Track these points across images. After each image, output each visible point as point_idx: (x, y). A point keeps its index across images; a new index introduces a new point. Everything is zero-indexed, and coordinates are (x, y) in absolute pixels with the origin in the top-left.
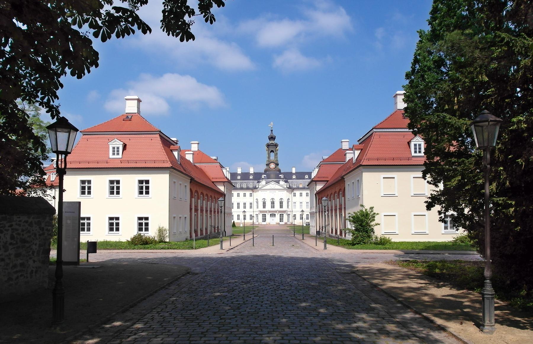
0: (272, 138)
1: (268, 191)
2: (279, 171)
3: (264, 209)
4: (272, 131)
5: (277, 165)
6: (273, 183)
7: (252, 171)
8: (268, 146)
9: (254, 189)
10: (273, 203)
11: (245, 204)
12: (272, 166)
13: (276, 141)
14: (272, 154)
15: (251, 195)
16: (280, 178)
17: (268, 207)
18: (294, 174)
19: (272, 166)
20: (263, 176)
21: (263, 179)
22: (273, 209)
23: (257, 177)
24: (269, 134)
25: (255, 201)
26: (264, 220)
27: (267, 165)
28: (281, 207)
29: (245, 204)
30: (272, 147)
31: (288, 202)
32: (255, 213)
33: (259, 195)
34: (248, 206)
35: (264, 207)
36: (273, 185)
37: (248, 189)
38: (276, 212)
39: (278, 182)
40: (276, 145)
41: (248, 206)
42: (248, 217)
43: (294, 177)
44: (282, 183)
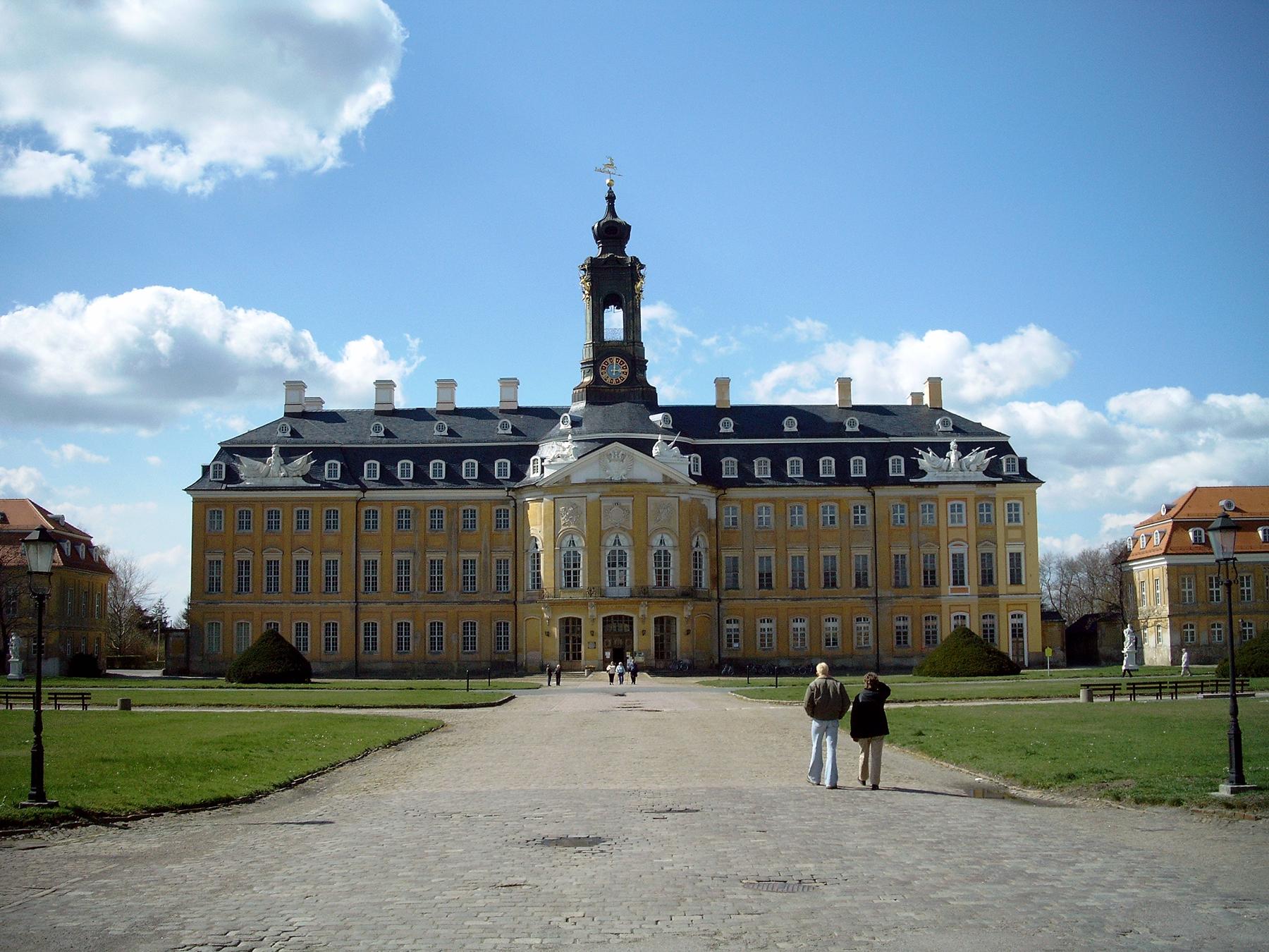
4: (611, 198)
5: (637, 364)
13: (631, 250)
14: (614, 319)
16: (653, 428)
19: (615, 371)
20: (564, 426)
21: (563, 435)
24: (599, 213)
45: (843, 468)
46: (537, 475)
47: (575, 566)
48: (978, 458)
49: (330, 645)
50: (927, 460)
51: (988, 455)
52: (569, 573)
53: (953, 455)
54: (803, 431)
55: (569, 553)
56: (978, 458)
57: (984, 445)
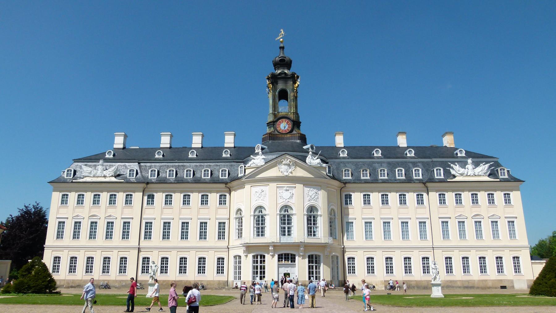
0: (284, 63)
1: (273, 185)
2: (303, 139)
5: (296, 124)
6: (289, 159)
8: (274, 79)
10: (286, 220)
11: (203, 225)
12: (284, 126)
13: (293, 69)
15: (222, 201)
17: (272, 233)
18: (341, 148)
19: (284, 126)
21: (258, 154)
22: (286, 239)
23: (242, 154)
25: (233, 215)
26: (259, 271)
27: (269, 124)
28: (311, 232)
29: (203, 225)
30: (282, 78)
31: (331, 223)
32: (233, 253)
34: (212, 230)
35: (260, 231)
36: (284, 168)
37: (215, 181)
38: (297, 246)
39: (303, 159)
40: (294, 78)
41: (212, 230)
42: (211, 265)
43: (344, 154)
44: (313, 161)
45: (408, 174)
46: (242, 175)
47: (262, 224)
48: (483, 168)
50: (456, 169)
51: (490, 167)
52: (259, 228)
53: (470, 166)
54: (384, 156)
55: (259, 217)
56: (483, 168)
57: (487, 163)
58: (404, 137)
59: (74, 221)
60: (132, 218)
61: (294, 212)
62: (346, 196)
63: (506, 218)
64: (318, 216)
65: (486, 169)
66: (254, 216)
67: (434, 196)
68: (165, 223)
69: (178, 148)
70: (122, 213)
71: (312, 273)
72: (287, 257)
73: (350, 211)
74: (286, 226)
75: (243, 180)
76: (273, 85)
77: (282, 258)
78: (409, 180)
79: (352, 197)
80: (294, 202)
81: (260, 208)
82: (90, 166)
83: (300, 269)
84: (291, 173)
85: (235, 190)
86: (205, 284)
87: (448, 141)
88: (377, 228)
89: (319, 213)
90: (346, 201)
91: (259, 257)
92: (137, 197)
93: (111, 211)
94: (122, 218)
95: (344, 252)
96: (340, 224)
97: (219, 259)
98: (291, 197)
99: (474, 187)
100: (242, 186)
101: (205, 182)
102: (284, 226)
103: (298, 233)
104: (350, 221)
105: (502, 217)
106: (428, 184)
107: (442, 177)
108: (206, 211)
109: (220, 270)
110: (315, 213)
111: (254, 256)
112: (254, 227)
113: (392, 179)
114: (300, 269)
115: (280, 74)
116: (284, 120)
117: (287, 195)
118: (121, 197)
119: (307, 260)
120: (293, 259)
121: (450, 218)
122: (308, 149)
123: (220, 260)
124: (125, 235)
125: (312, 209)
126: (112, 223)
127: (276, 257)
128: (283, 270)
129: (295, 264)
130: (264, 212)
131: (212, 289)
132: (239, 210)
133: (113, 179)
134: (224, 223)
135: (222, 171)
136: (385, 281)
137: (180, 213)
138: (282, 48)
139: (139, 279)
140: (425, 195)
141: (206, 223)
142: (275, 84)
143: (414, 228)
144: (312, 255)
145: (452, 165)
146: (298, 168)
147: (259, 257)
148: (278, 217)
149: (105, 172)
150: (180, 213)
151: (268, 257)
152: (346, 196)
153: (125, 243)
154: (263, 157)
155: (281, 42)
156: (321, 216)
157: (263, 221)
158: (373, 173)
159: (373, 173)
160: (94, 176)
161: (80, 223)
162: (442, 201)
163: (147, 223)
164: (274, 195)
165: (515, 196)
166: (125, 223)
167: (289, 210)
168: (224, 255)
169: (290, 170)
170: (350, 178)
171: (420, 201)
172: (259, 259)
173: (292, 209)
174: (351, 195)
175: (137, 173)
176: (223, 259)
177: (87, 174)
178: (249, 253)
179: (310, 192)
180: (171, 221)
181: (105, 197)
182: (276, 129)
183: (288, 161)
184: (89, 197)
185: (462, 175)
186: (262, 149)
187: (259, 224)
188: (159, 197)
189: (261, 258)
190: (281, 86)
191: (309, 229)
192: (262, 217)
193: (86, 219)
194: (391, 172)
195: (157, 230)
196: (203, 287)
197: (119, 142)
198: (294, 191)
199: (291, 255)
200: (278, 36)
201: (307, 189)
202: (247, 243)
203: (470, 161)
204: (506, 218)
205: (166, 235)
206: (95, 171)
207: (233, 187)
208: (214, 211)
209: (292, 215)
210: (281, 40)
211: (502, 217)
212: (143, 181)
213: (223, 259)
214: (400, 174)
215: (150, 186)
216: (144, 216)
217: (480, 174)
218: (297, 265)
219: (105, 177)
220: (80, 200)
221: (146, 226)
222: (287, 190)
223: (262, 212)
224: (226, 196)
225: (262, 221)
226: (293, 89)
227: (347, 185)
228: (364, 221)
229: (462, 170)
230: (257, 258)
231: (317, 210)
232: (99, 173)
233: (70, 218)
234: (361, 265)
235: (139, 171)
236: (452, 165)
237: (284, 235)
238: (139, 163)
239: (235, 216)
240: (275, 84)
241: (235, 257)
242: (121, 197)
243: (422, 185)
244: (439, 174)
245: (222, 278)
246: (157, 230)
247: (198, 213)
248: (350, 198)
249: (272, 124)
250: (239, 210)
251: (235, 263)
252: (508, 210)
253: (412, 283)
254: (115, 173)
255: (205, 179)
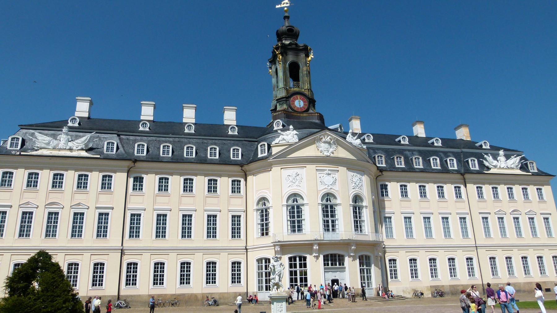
0: (291, 33)
1: (312, 167)
3: (297, 237)
5: (311, 102)
7: (230, 117)
9: (249, 164)
10: (329, 211)
15: (236, 188)
17: (312, 228)
19: (299, 103)
22: (330, 236)
25: (253, 206)
26: (298, 278)
28: (358, 225)
33: (271, 185)
34: (224, 226)
38: (346, 244)
41: (224, 226)
42: (223, 273)
45: (444, 164)
46: (266, 154)
47: (298, 217)
48: (515, 161)
49: (97, 280)
50: (489, 161)
51: (521, 159)
52: (294, 222)
53: (502, 158)
55: (293, 208)
56: (515, 161)
57: (518, 155)
58: (422, 126)
59: (21, 210)
60: (112, 208)
61: (338, 201)
62: (382, 185)
63: (541, 214)
64: (363, 207)
65: (518, 161)
66: (287, 206)
67: (472, 188)
68: (159, 215)
69: (165, 123)
70: (97, 201)
71: (365, 276)
72: (333, 260)
73: (387, 204)
74: (330, 219)
75: (271, 160)
76: (282, 56)
77: (336, 261)
78: (445, 170)
79: (389, 187)
80: (337, 189)
81: (295, 196)
82: (46, 135)
83: (350, 275)
84: (333, 153)
85: (253, 175)
86: (217, 298)
87: (463, 134)
88: (418, 224)
89: (364, 204)
90: (382, 192)
91: (298, 259)
92: (119, 179)
93: (80, 197)
94: (97, 208)
95: (385, 252)
96: (381, 218)
97: (233, 263)
98: (334, 183)
99: (509, 180)
100: (268, 168)
101: (212, 162)
102: (327, 219)
103: (344, 230)
104: (387, 215)
105: (538, 214)
106: (467, 176)
107: (477, 168)
108: (214, 200)
109: (236, 278)
110: (360, 204)
111: (290, 259)
112: (288, 220)
113: (428, 168)
114: (350, 275)
115: (290, 44)
116: (299, 96)
117: (328, 180)
118: (95, 178)
119: (358, 261)
120: (342, 262)
121: (490, 213)
122: (337, 129)
123: (236, 265)
124: (102, 231)
125: (357, 198)
126: (82, 214)
127: (321, 258)
128: (332, 276)
129: (345, 268)
130: (300, 201)
131: (226, 304)
132: (263, 200)
133: (84, 154)
134: (239, 217)
135: (234, 150)
136: (431, 287)
137: (180, 203)
138: (286, 18)
139: (122, 293)
140: (462, 187)
141: (215, 216)
142: (285, 55)
143: (454, 224)
144: (362, 256)
145: (485, 156)
146: (340, 148)
147: (298, 259)
148: (320, 208)
149: (70, 144)
150: (180, 203)
151: (310, 259)
152: (382, 185)
153: (101, 243)
154: (295, 132)
155: (286, 11)
156: (366, 207)
157: (299, 212)
158: (408, 162)
159: (408, 162)
160: (54, 149)
161: (31, 213)
162: (480, 195)
163: (132, 215)
164: (305, 181)
165: (547, 190)
166: (101, 214)
167: (332, 199)
168: (241, 258)
169: (331, 150)
170: (384, 165)
171: (458, 195)
172: (298, 262)
173: (335, 197)
174: (387, 185)
175: (118, 148)
176: (239, 263)
177: (43, 145)
178: (284, 253)
179: (355, 177)
180: (168, 213)
181: (70, 177)
182: (289, 106)
183: (328, 138)
184: (46, 177)
185: (495, 167)
186: (283, 126)
187: (294, 217)
188: (151, 181)
189: (300, 260)
190: (291, 58)
191: (356, 222)
192: (298, 207)
193: (42, 208)
194: (427, 162)
195: (148, 225)
196: (215, 302)
197: (82, 109)
198: (337, 175)
199: (339, 256)
200: (280, 4)
201: (351, 174)
202: (279, 242)
203: (501, 152)
204: (541, 214)
205: (161, 232)
206: (54, 143)
207: (250, 171)
208: (225, 201)
209: (336, 205)
210: (286, 9)
211: (538, 214)
212: (128, 158)
213: (239, 263)
214: (435, 163)
215: (138, 164)
216: (128, 206)
217: (512, 166)
218: (347, 269)
219: (71, 150)
220: (32, 181)
221: (131, 220)
222: (329, 174)
223: (297, 202)
224: (240, 181)
225: (298, 212)
226: (306, 63)
227: (384, 173)
228: (403, 216)
229: (495, 163)
230: (295, 260)
231: (362, 200)
232: (61, 145)
233: (15, 207)
234: (403, 268)
235: (120, 146)
236: (485, 156)
237: (328, 230)
238: (119, 135)
239: (255, 207)
240: (285, 55)
241: (259, 261)
242: (95, 178)
243: (459, 176)
244: (474, 165)
245: (240, 288)
246: (148, 225)
247: (205, 203)
248: (386, 189)
249: (286, 99)
250: (263, 200)
251: (260, 268)
252: (542, 205)
253: (459, 288)
254: (86, 145)
255: (212, 159)
